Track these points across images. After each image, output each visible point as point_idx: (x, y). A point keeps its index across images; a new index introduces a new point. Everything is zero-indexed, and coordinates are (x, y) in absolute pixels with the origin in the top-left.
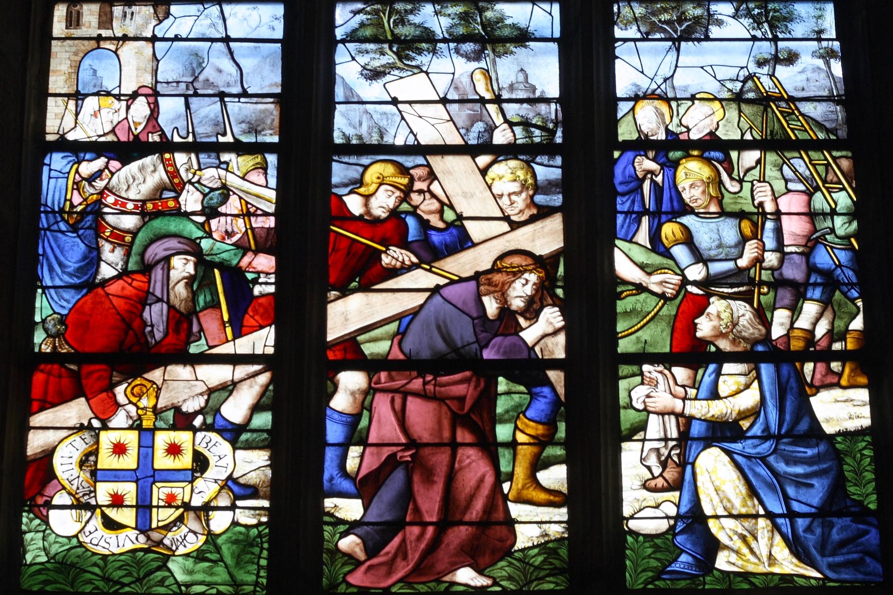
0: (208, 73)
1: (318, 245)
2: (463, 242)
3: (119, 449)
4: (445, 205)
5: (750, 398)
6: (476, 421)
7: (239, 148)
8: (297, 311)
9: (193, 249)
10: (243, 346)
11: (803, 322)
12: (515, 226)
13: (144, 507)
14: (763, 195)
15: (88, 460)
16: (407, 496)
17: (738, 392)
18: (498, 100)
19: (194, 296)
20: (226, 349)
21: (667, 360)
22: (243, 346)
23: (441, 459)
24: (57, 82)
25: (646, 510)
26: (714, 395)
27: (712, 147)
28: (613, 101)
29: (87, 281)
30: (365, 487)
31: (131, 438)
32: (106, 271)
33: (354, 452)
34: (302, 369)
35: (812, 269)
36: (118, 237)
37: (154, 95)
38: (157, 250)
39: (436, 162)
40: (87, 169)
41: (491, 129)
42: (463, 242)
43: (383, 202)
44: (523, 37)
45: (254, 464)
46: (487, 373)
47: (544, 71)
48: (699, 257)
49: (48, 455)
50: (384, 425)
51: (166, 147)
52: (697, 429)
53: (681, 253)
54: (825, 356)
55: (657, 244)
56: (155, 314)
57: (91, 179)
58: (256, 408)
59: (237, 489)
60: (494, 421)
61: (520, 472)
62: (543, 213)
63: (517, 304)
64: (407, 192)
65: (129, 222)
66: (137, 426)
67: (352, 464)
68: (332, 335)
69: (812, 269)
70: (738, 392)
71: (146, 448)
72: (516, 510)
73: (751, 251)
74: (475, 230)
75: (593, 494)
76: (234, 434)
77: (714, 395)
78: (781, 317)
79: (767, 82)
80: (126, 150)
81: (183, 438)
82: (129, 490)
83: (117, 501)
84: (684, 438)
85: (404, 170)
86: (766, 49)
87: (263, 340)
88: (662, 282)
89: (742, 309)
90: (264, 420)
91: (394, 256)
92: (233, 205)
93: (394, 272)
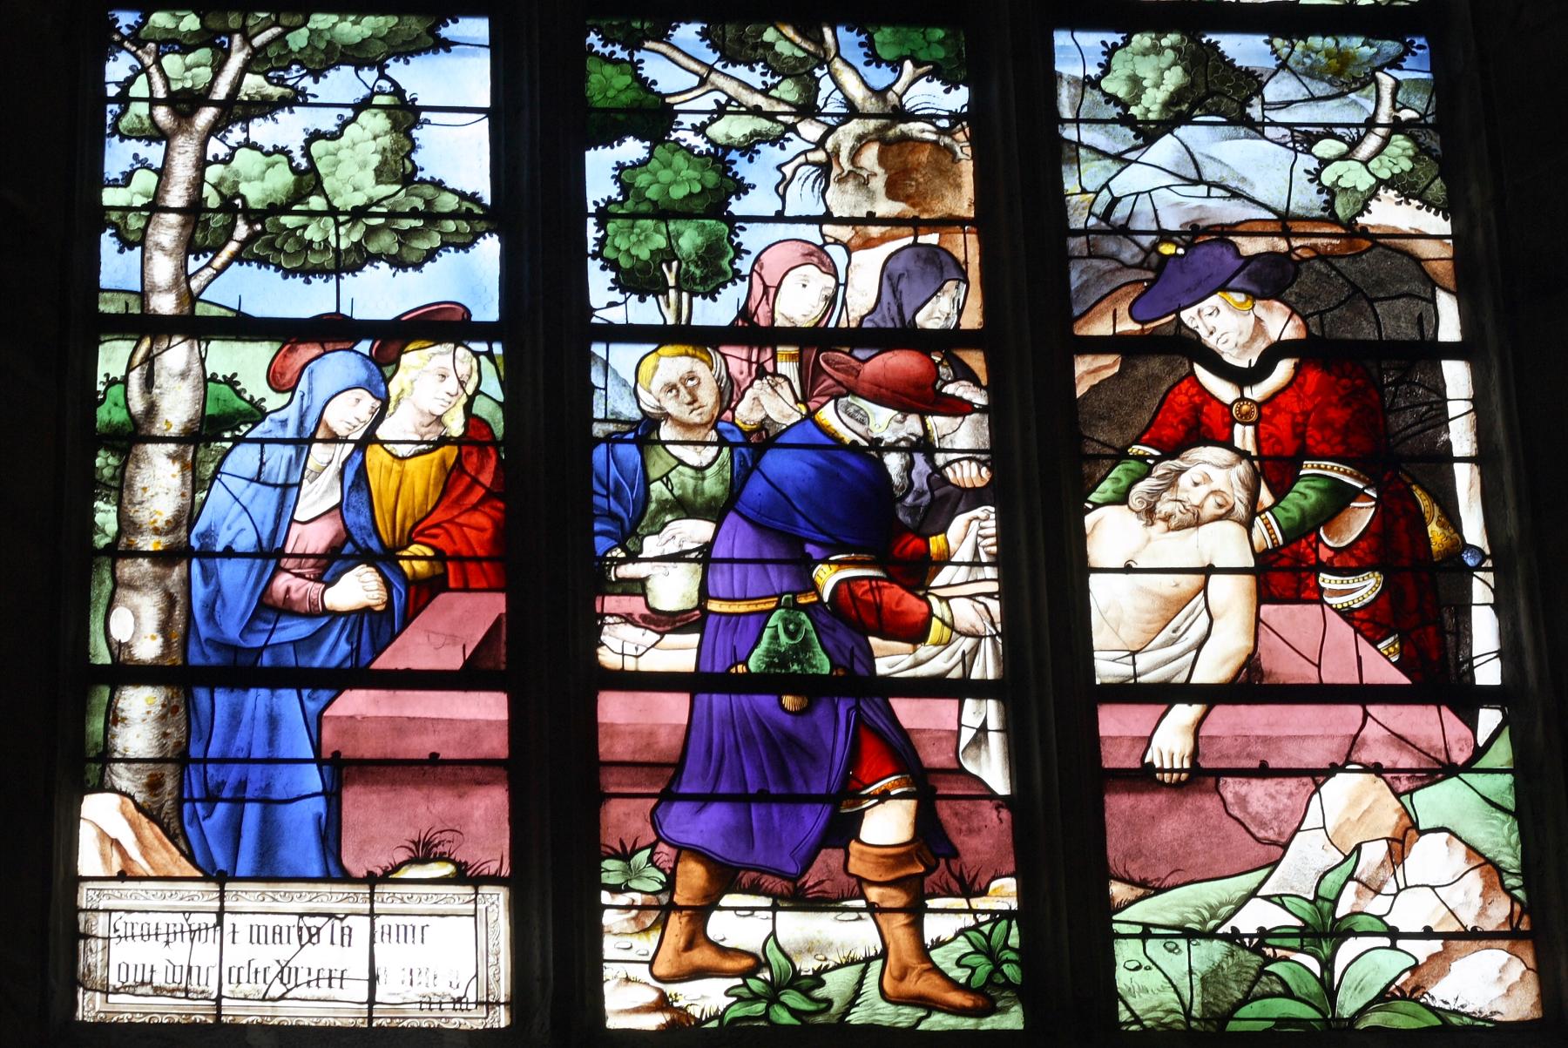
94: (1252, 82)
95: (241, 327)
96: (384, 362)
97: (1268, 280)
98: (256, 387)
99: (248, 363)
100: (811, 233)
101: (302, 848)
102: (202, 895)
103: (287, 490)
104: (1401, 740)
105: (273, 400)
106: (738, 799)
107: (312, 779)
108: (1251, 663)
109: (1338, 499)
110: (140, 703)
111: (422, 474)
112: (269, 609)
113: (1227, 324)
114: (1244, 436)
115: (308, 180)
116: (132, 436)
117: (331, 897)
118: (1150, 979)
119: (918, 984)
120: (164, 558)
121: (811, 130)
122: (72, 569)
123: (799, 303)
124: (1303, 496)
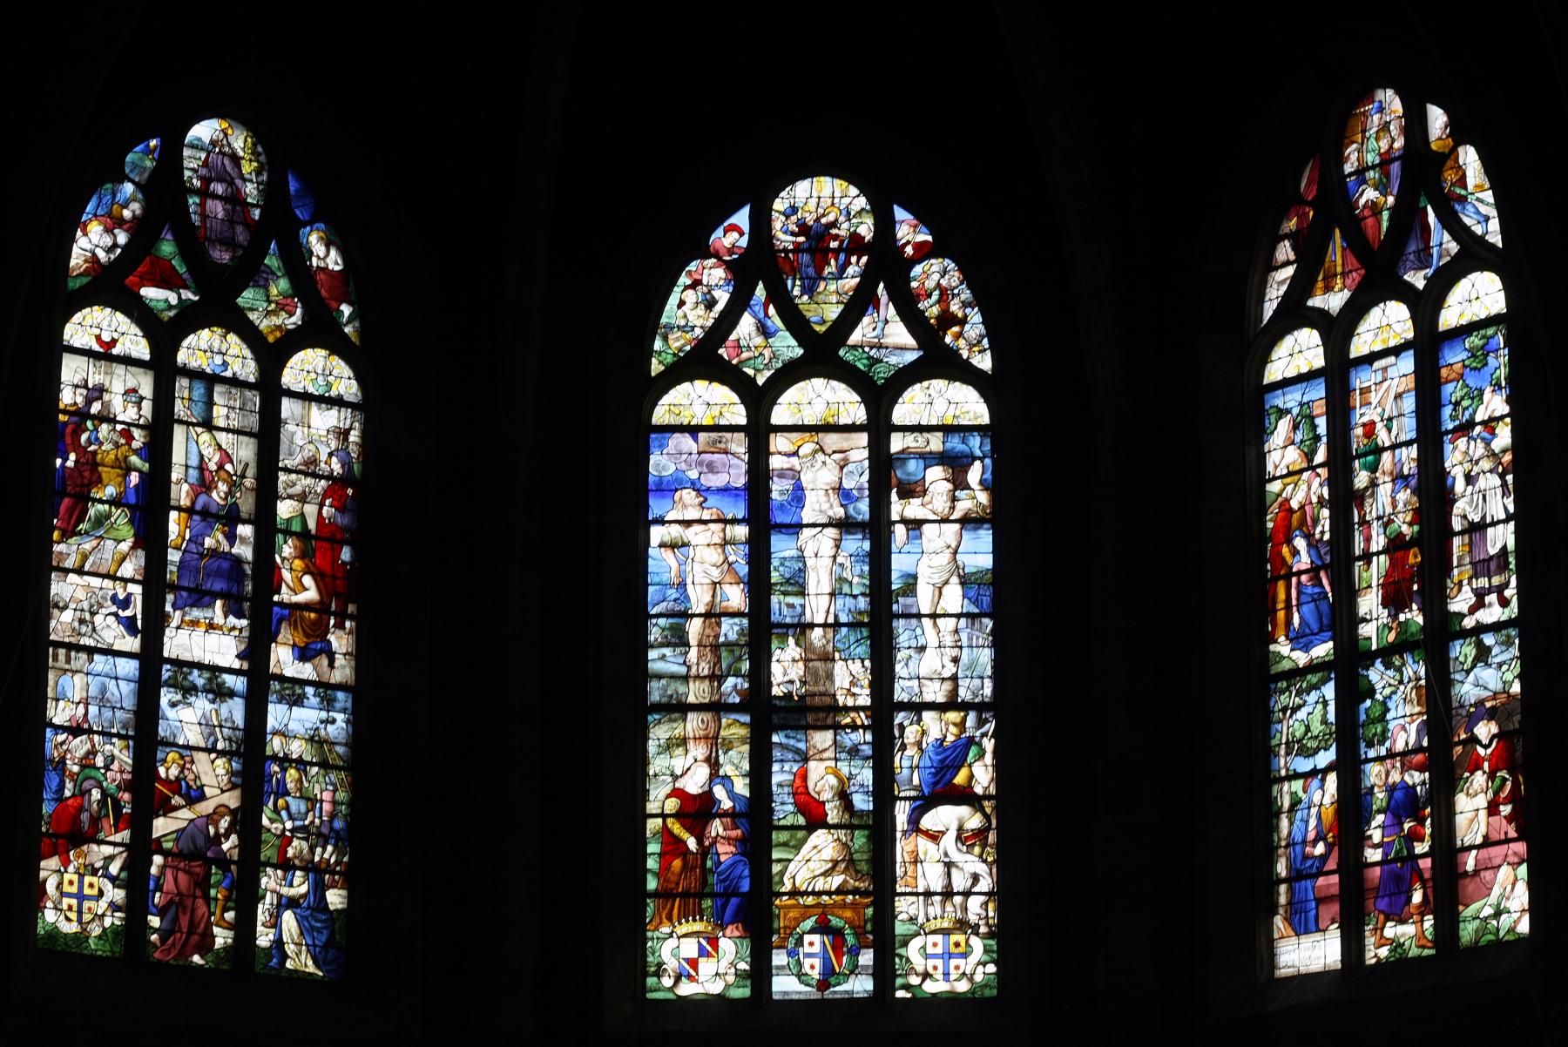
0: (108, 695)
1: (148, 793)
2: (202, 797)
3: (71, 883)
4: (197, 777)
5: (304, 889)
6: (203, 884)
7: (118, 736)
8: (140, 824)
9: (100, 786)
10: (117, 838)
11: (326, 856)
12: (223, 791)
13: (80, 912)
14: (317, 791)
15: (59, 885)
16: (176, 919)
17: (300, 886)
18: (221, 726)
19: (100, 809)
20: (111, 839)
21: (276, 867)
22: (117, 838)
23: (189, 902)
24: (50, 694)
25: (264, 939)
26: (291, 885)
27: (301, 764)
28: (266, 733)
29: (60, 798)
30: (161, 913)
31: (75, 878)
32: (67, 793)
33: (158, 895)
34: (141, 848)
35: (332, 829)
36: (72, 775)
37: (86, 703)
38: (86, 785)
39: (195, 754)
40: (61, 738)
41: (216, 740)
42: (202, 797)
43: (174, 772)
44: (232, 694)
45: (119, 895)
46: (208, 863)
47: (236, 710)
48: (291, 817)
49: (45, 881)
50: (169, 884)
51: (90, 731)
52: (284, 901)
53: (284, 813)
54: (333, 873)
55: (276, 810)
56: (85, 817)
57: (63, 743)
58: (122, 869)
59: (114, 907)
60: (210, 886)
61: (218, 912)
62: (234, 787)
63: (222, 831)
64: (183, 768)
65: (76, 769)
66: (77, 872)
67: (156, 900)
68: (155, 836)
69: (332, 829)
70: (300, 886)
71: (81, 883)
72: (216, 930)
73: (310, 818)
74: (208, 791)
75: (244, 928)
76: (114, 880)
77: (291, 885)
78: (319, 850)
79: (323, 732)
80: (75, 730)
81: (95, 880)
82: (74, 902)
83: (70, 908)
84: (279, 905)
85: (182, 757)
86: (324, 715)
87: (124, 836)
88: (276, 827)
89: (304, 845)
90: (123, 875)
91: (177, 800)
92: (115, 766)
93: (176, 808)
94: (1489, 649)
95: (1296, 776)
96: (1323, 780)
97: (1492, 714)
98: (1300, 793)
99: (1297, 785)
100: (1401, 721)
101: (1312, 925)
102: (1294, 940)
103: (1307, 822)
104: (1515, 854)
105: (1304, 796)
106: (1390, 895)
107: (1313, 904)
108: (1486, 837)
109: (1504, 780)
110: (1283, 888)
111: (1331, 811)
112: (1306, 857)
113: (1485, 730)
114: (1486, 765)
115: (1308, 728)
116: (1279, 812)
117: (1318, 936)
118: (1467, 931)
119: (1423, 942)
120: (1287, 847)
121: (1402, 688)
122: (1269, 854)
123: (1400, 746)
124: (1498, 781)
